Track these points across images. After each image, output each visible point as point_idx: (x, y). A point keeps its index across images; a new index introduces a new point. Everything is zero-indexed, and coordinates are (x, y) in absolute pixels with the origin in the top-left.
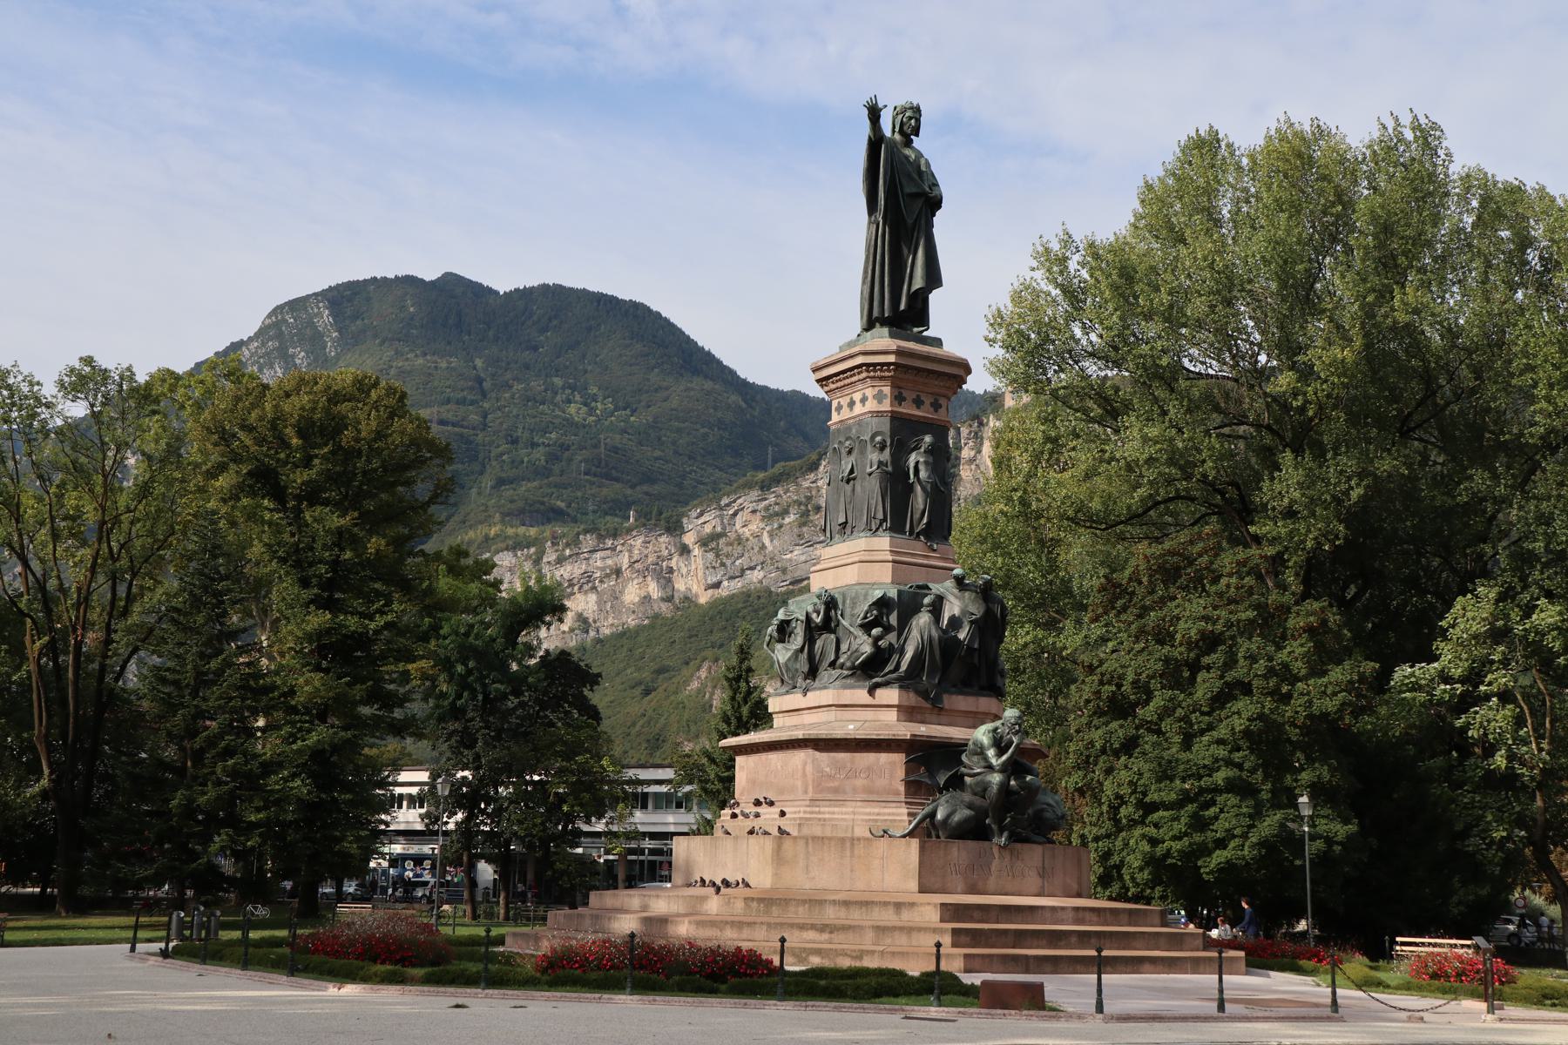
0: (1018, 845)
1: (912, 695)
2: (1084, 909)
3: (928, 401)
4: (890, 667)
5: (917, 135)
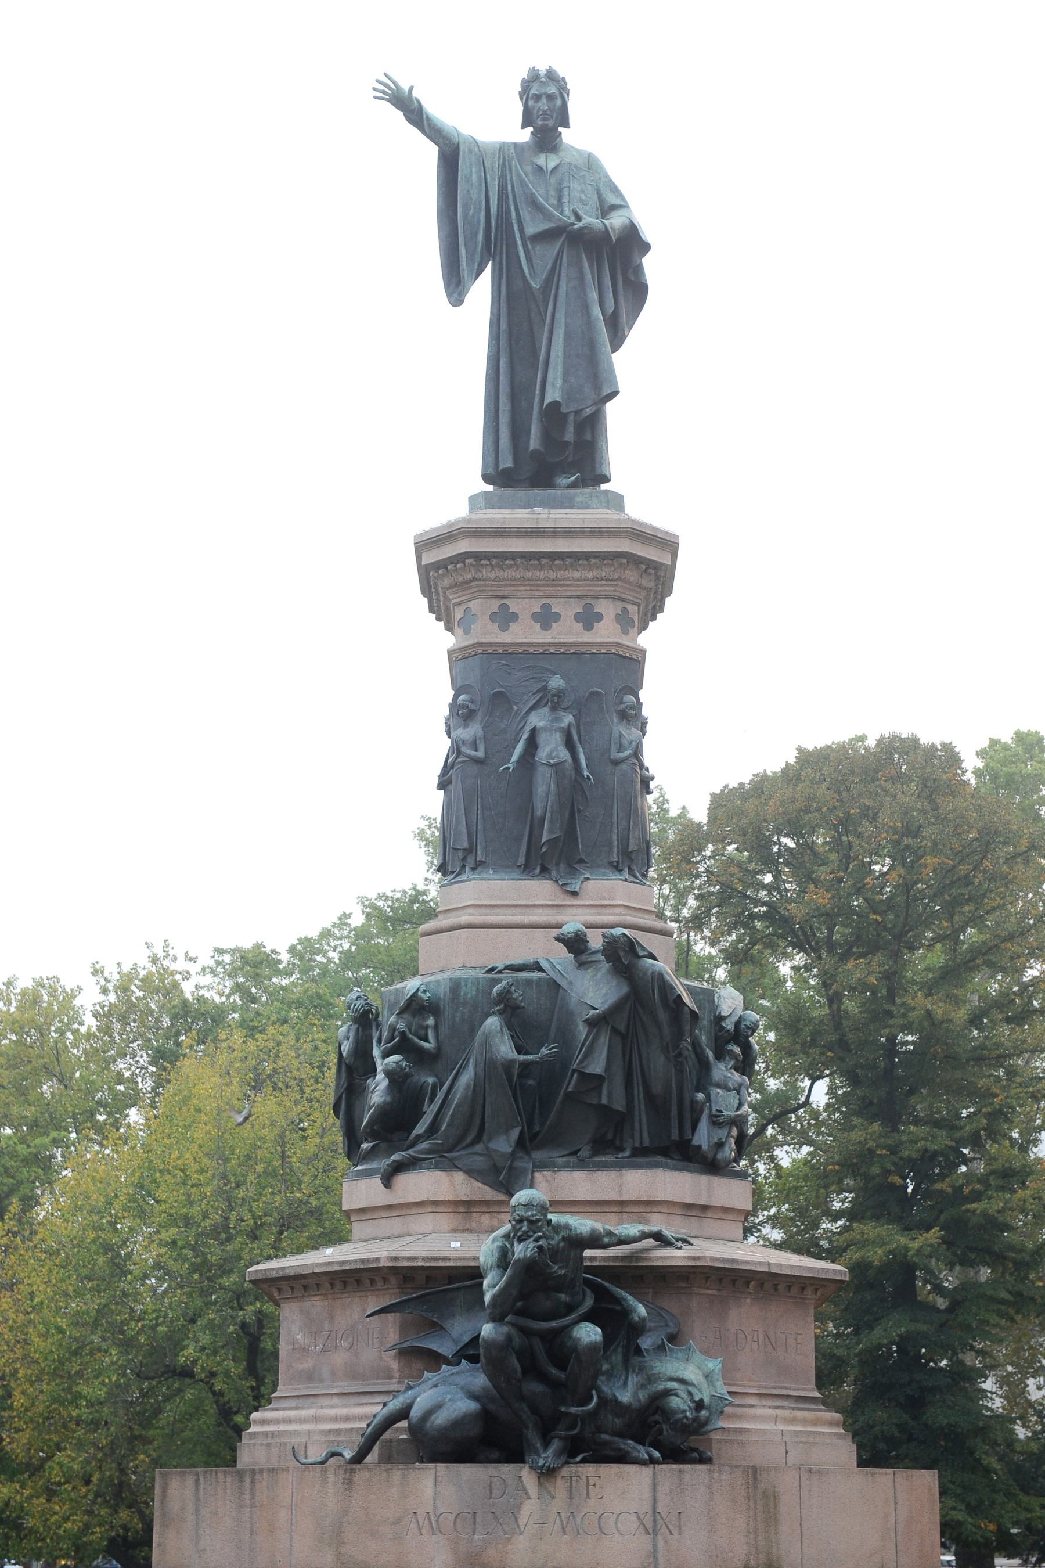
0: (590, 1469)
1: (459, 1177)
3: (567, 610)
4: (420, 1129)
5: (566, 124)
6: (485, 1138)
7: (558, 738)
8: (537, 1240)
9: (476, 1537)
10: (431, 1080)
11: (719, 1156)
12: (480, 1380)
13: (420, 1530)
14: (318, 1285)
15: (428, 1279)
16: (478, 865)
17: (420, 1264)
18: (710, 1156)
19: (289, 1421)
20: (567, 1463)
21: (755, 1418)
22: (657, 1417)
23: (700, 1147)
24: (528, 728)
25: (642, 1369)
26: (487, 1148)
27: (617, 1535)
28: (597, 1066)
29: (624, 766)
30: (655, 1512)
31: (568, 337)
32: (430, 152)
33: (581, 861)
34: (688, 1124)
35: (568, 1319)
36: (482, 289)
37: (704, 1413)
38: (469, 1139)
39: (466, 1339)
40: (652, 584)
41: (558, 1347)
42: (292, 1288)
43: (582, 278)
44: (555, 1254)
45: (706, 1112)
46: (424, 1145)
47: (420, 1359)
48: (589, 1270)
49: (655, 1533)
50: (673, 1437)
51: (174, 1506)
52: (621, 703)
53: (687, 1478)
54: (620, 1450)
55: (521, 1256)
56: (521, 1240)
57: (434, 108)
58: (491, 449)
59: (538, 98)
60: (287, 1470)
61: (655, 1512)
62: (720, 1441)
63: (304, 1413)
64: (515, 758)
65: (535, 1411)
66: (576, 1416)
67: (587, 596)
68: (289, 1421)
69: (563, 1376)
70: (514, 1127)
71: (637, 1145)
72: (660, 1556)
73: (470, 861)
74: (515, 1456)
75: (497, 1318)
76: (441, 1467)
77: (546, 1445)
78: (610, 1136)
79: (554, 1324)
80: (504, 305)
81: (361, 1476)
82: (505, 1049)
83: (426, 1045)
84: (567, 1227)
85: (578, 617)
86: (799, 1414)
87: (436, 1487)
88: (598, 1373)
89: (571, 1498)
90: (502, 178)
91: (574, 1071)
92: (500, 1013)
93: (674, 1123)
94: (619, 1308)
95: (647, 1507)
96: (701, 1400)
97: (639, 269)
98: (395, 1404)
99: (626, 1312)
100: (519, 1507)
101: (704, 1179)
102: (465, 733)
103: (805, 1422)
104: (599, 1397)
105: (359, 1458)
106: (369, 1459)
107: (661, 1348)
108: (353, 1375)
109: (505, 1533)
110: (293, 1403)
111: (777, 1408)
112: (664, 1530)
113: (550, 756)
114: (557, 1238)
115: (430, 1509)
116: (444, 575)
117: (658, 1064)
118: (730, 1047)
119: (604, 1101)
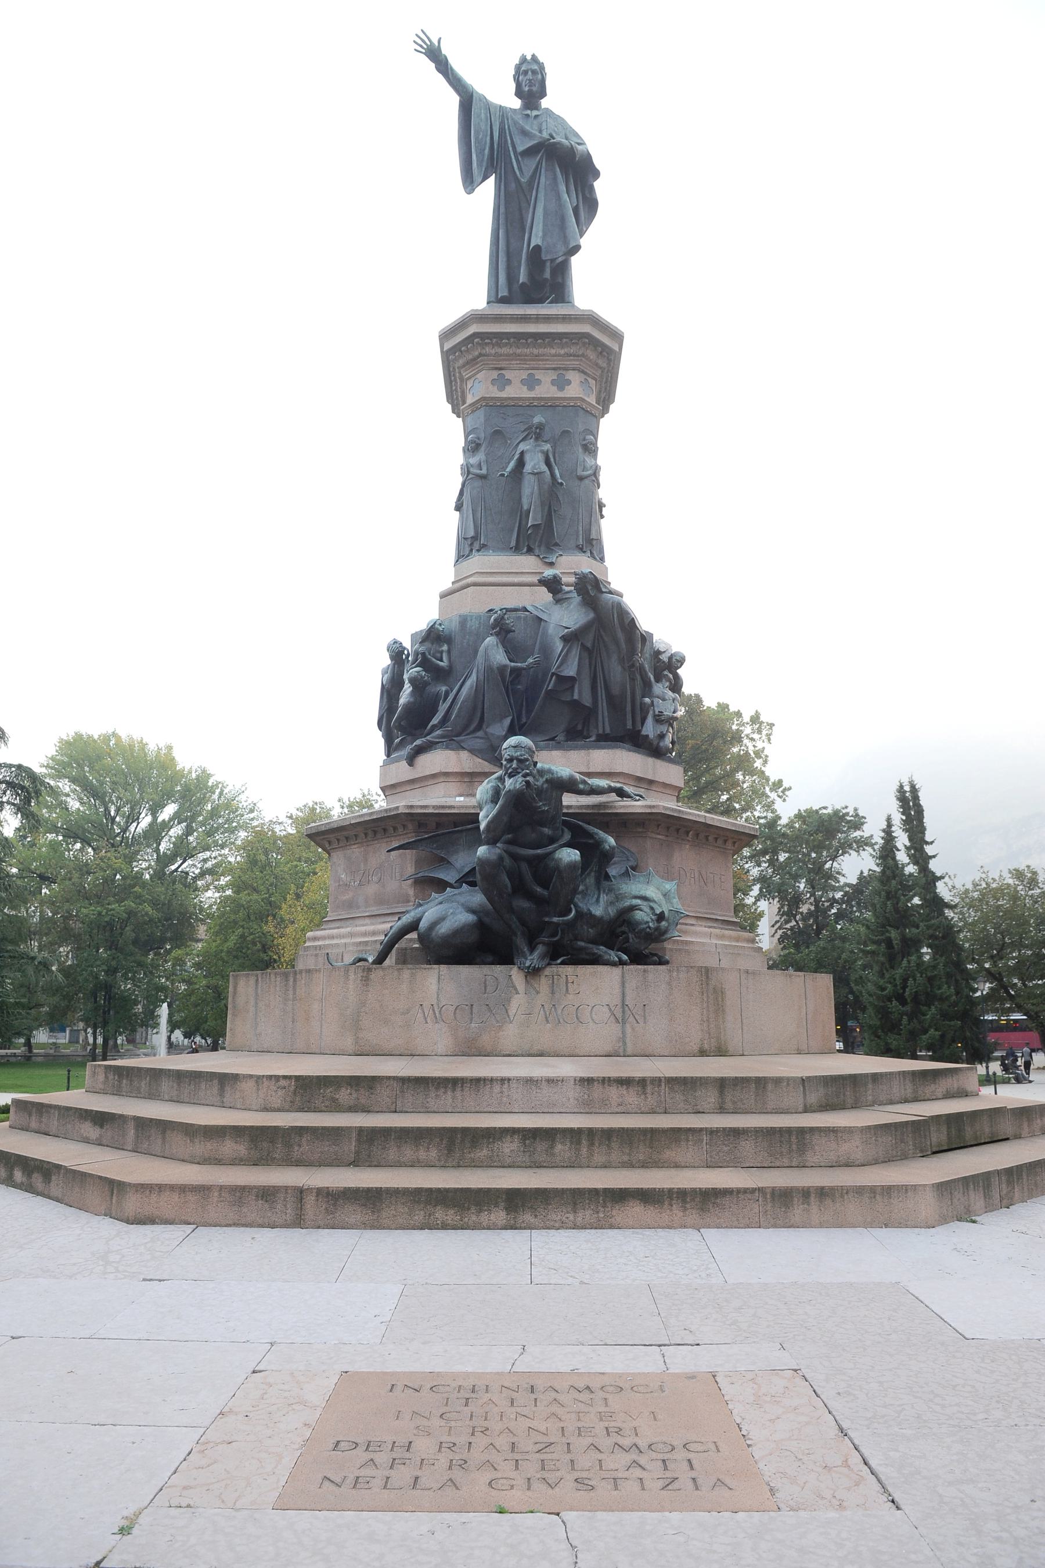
0: (569, 969)
1: (464, 755)
2: (606, 1081)
4: (435, 721)
6: (484, 726)
7: (541, 457)
8: (525, 776)
9: (473, 1025)
10: (444, 689)
11: (661, 744)
12: (478, 898)
13: (425, 1019)
14: (356, 836)
15: (438, 825)
16: (483, 547)
17: (431, 811)
18: (655, 743)
19: (332, 937)
20: (549, 964)
21: (696, 934)
22: (624, 928)
23: (647, 736)
24: (518, 452)
25: (611, 890)
26: (486, 733)
27: (591, 1024)
28: (571, 671)
29: (586, 481)
30: (624, 1004)
31: (546, 214)
32: (453, 100)
33: (556, 544)
34: (638, 719)
35: (550, 848)
36: (488, 188)
37: (664, 923)
38: (472, 727)
39: (467, 870)
40: (605, 365)
41: (544, 870)
42: (338, 840)
43: (555, 178)
44: (540, 792)
45: (651, 712)
46: (439, 732)
47: (429, 885)
48: (565, 815)
49: (624, 1022)
50: (637, 943)
51: (241, 1000)
52: (584, 439)
53: (651, 977)
54: (594, 954)
55: (512, 788)
56: (510, 776)
57: (456, 64)
58: (494, 286)
59: (526, 73)
60: (319, 970)
61: (624, 1004)
62: (671, 950)
63: (342, 930)
64: (509, 469)
65: (523, 923)
66: (557, 924)
67: (560, 368)
68: (332, 937)
69: (546, 893)
70: (507, 717)
71: (601, 732)
72: (628, 1040)
73: (476, 546)
74: (506, 958)
75: (492, 842)
76: (444, 968)
77: (532, 950)
78: (580, 727)
79: (539, 851)
80: (502, 202)
81: (377, 974)
82: (500, 657)
83: (441, 664)
84: (550, 771)
85: (553, 383)
86: (727, 932)
87: (441, 984)
88: (575, 891)
89: (553, 993)
90: (502, 123)
91: (553, 674)
92: (497, 634)
93: (629, 716)
94: (591, 841)
95: (617, 1000)
96: (663, 912)
97: (592, 189)
98: (406, 919)
99: (598, 844)
100: (509, 1001)
101: (650, 761)
102: (473, 461)
103: (730, 938)
104: (577, 911)
105: (380, 960)
106: (387, 962)
107: (626, 874)
108: (380, 901)
109: (498, 1022)
110: (337, 924)
111: (710, 927)
112: (631, 1019)
113: (534, 467)
114: (542, 780)
115: (434, 1002)
116: (459, 357)
117: (616, 672)
118: (666, 673)
119: (576, 697)
